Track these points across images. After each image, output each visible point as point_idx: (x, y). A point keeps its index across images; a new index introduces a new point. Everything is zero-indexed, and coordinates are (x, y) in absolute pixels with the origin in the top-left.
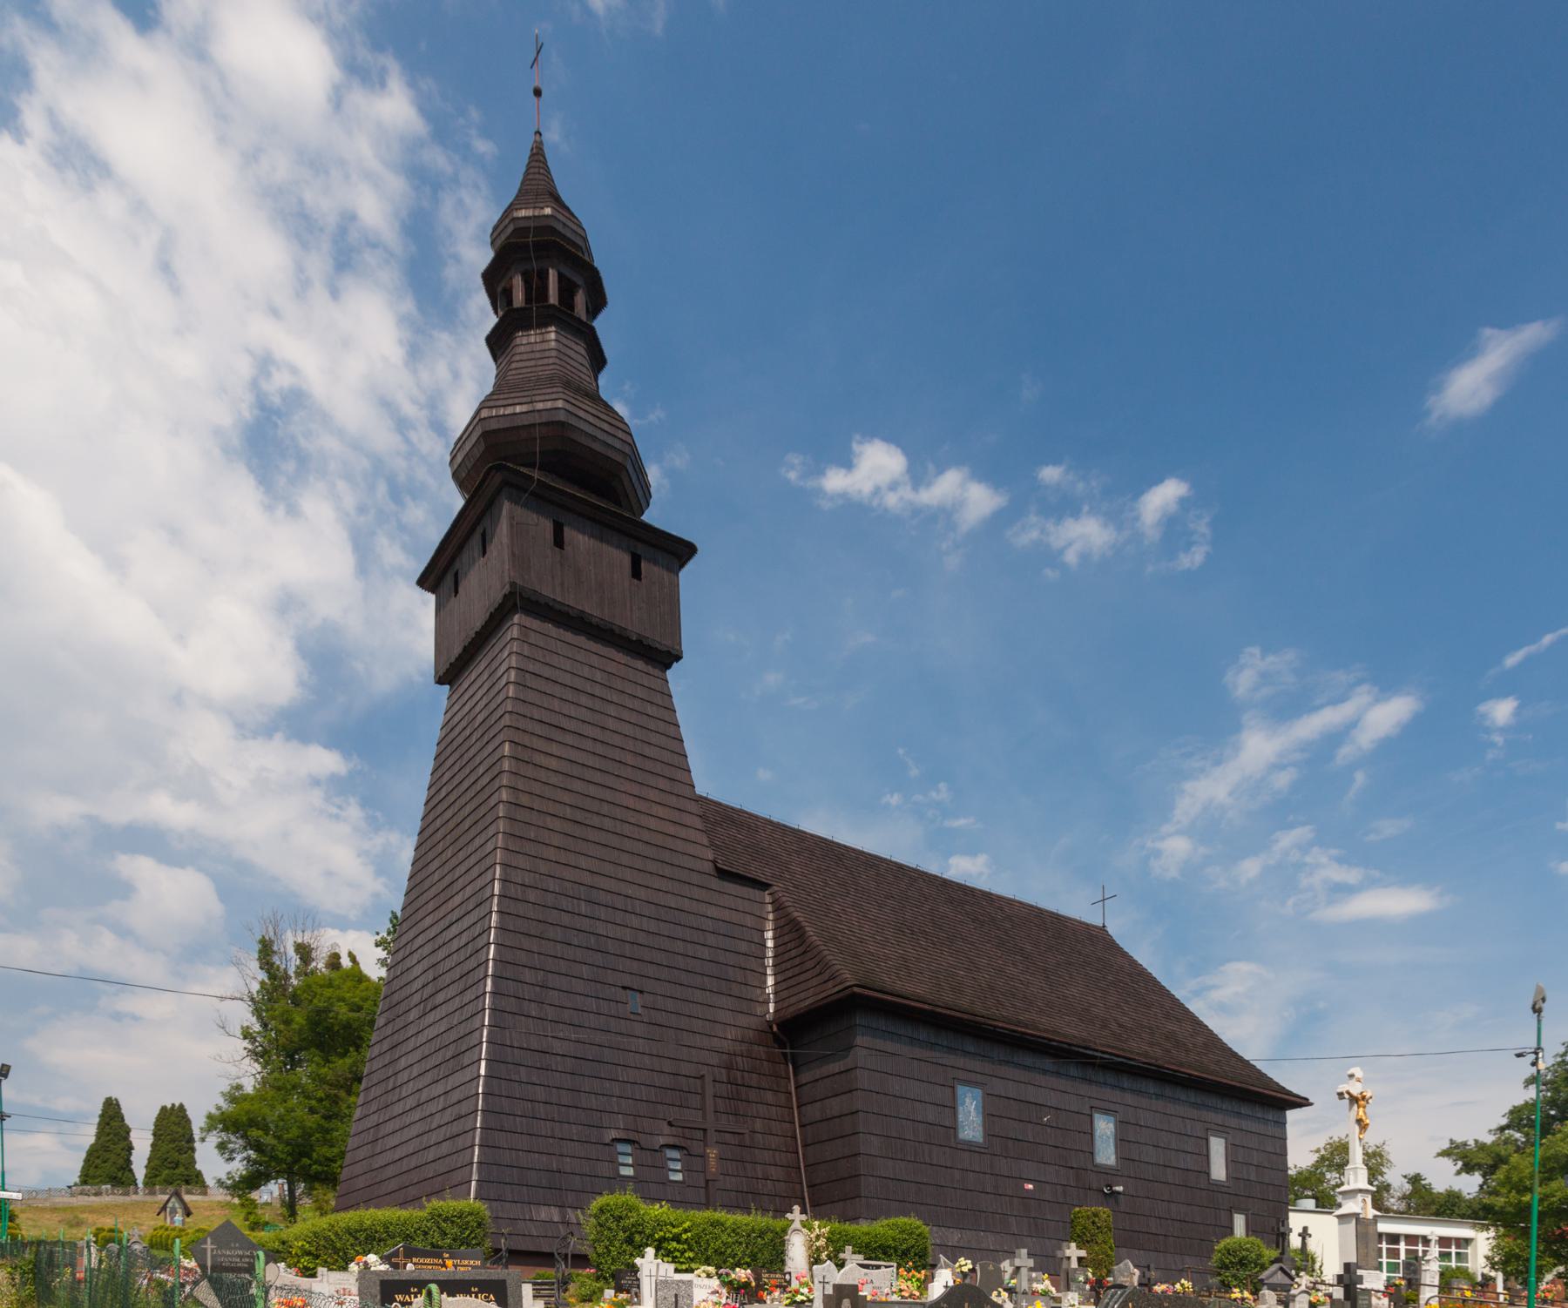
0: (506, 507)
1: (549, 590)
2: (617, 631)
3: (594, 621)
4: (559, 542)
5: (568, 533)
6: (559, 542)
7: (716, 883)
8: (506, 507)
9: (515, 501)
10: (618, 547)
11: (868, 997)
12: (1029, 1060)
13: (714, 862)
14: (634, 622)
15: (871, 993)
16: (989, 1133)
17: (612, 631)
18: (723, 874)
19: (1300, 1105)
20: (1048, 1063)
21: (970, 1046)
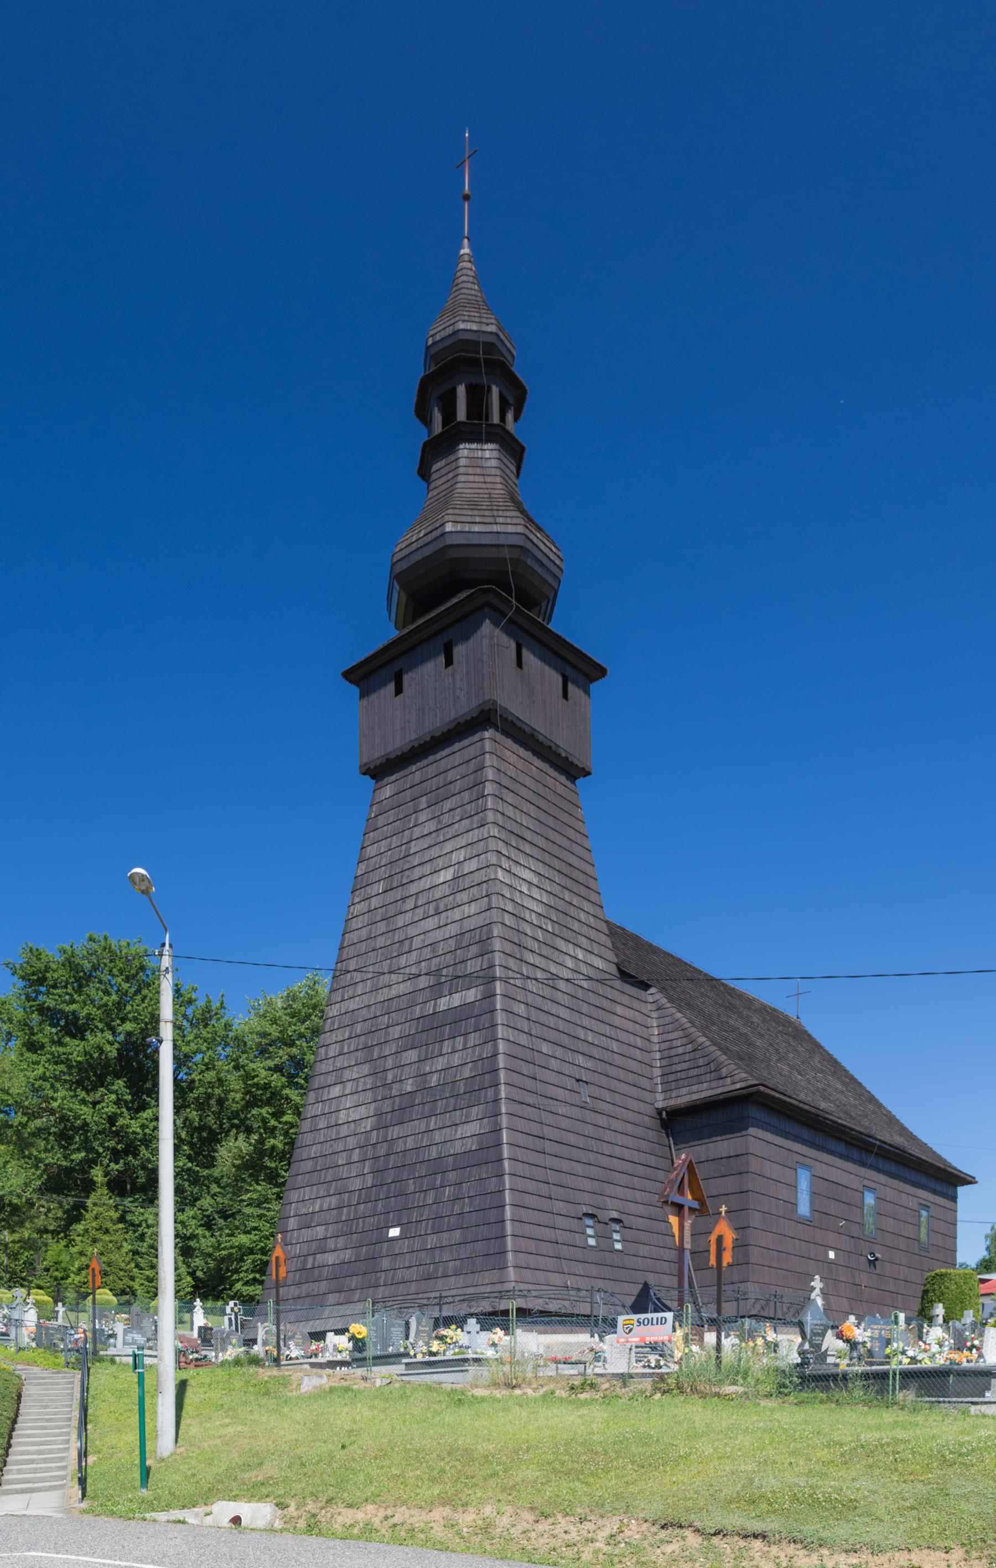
0: (487, 627)
1: (516, 708)
2: (554, 748)
3: (540, 738)
4: (520, 664)
5: (526, 654)
6: (520, 664)
7: (618, 984)
8: (487, 627)
9: (496, 624)
10: (555, 668)
11: (774, 1097)
12: (832, 1144)
13: (617, 965)
14: (562, 740)
15: (777, 1095)
16: (813, 1210)
17: (550, 747)
18: (624, 976)
19: (970, 1183)
20: (842, 1148)
21: (806, 1133)
